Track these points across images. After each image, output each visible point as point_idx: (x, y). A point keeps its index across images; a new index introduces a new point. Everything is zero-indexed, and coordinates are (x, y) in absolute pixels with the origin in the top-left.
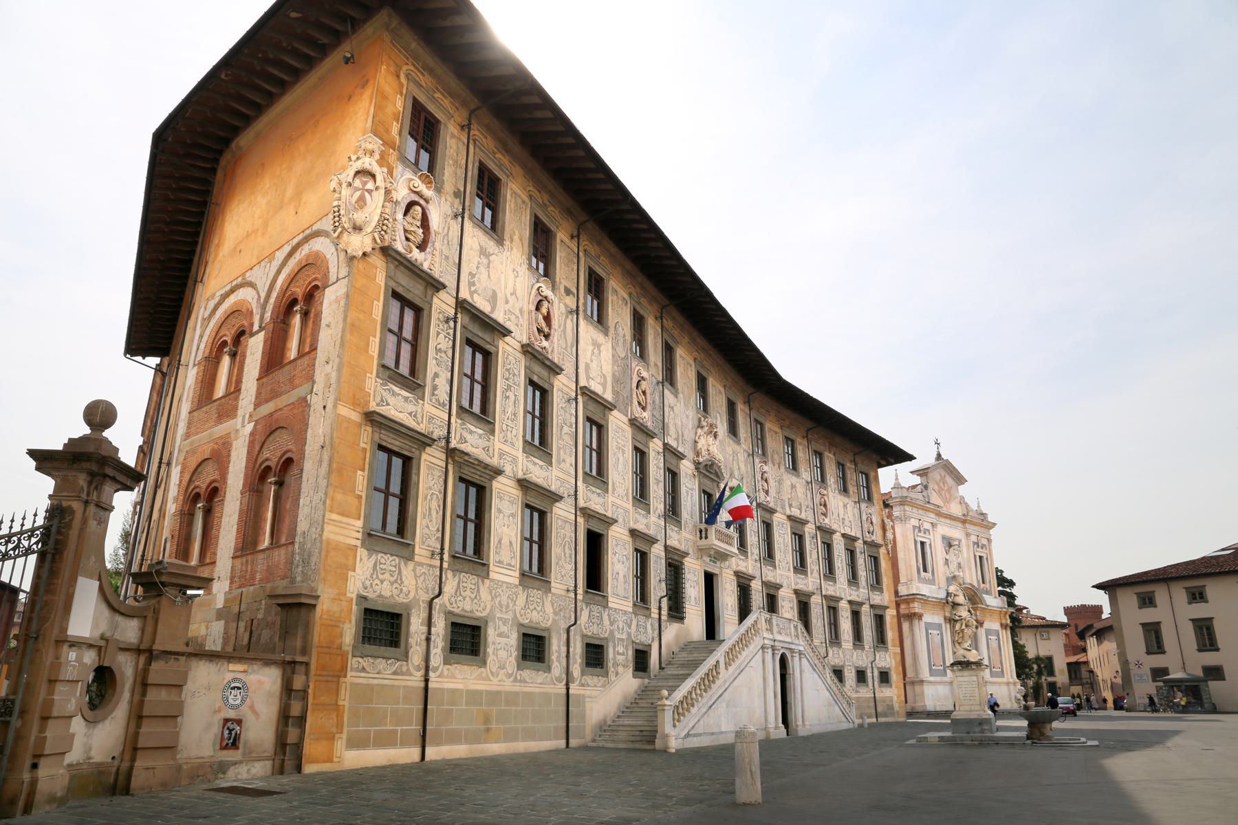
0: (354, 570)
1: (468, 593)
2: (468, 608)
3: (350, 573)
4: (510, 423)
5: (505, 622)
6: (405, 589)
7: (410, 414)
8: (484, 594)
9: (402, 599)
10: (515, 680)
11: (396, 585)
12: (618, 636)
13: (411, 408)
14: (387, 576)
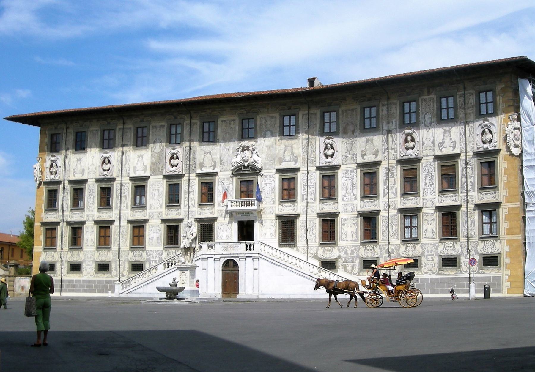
1: (75, 256)
5: (89, 261)
10: (95, 276)
12: (152, 259)
13: (55, 216)
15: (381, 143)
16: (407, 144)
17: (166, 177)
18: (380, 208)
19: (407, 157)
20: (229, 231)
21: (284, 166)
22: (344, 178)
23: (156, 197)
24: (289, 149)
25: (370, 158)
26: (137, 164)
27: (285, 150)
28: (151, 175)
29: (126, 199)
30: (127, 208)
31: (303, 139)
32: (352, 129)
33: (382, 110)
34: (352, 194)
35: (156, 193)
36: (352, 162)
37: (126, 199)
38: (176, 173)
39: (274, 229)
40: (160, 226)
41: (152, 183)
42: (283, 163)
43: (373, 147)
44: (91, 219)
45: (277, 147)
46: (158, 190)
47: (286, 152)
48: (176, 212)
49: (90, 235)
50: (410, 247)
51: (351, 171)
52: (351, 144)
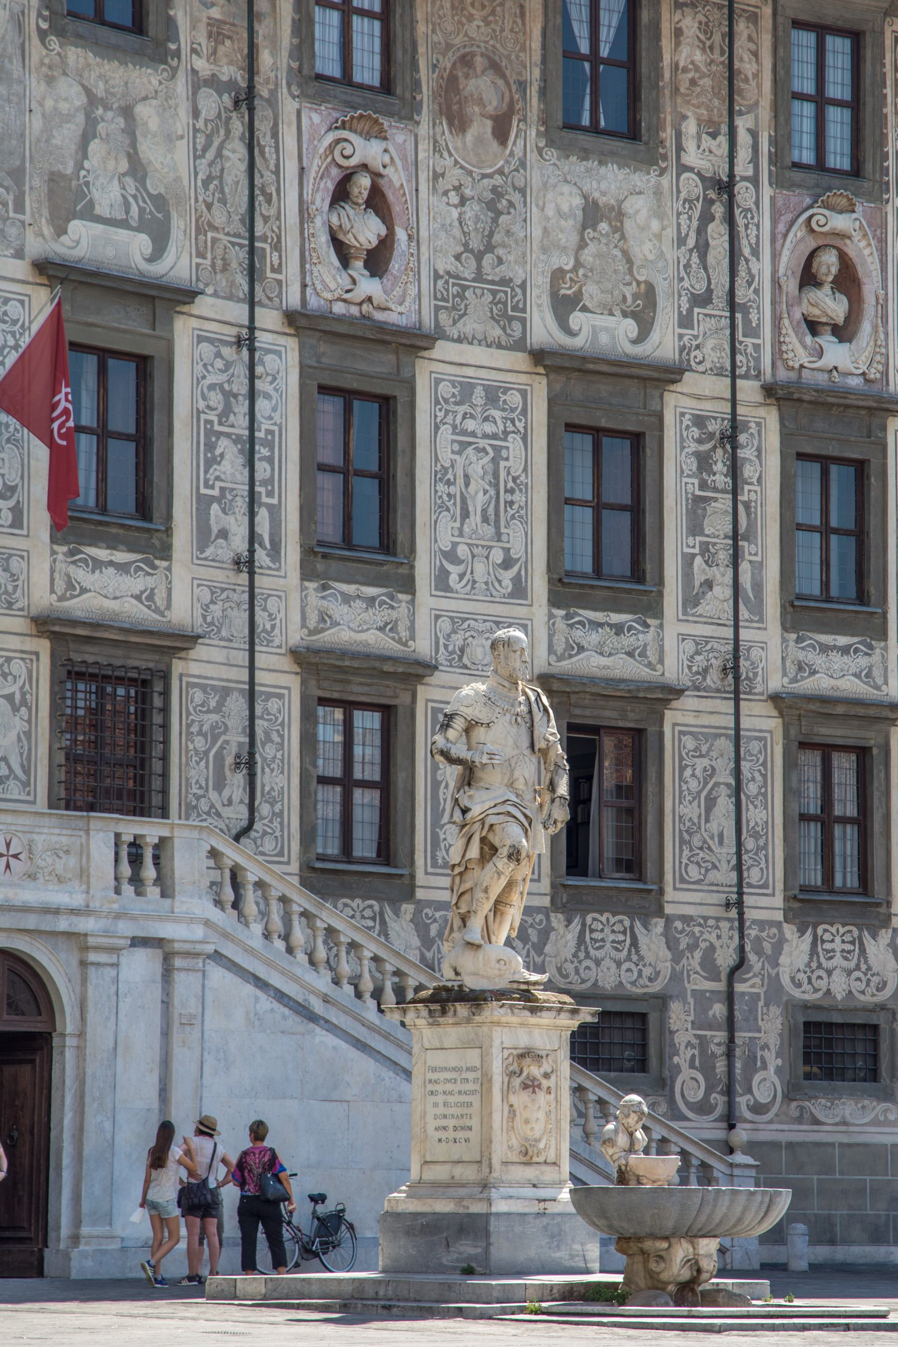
15: (671, 253)
16: (814, 294)
18: (672, 670)
19: (822, 379)
21: (83, 242)
22: (446, 432)
24: (111, 124)
25: (602, 331)
27: (91, 123)
31: (197, 83)
32: (493, 103)
33: (678, 33)
34: (497, 556)
36: (497, 332)
39: (18, 724)
42: (76, 227)
43: (622, 267)
45: (36, 86)
47: (94, 146)
50: (838, 945)
51: (493, 395)
52: (494, 205)
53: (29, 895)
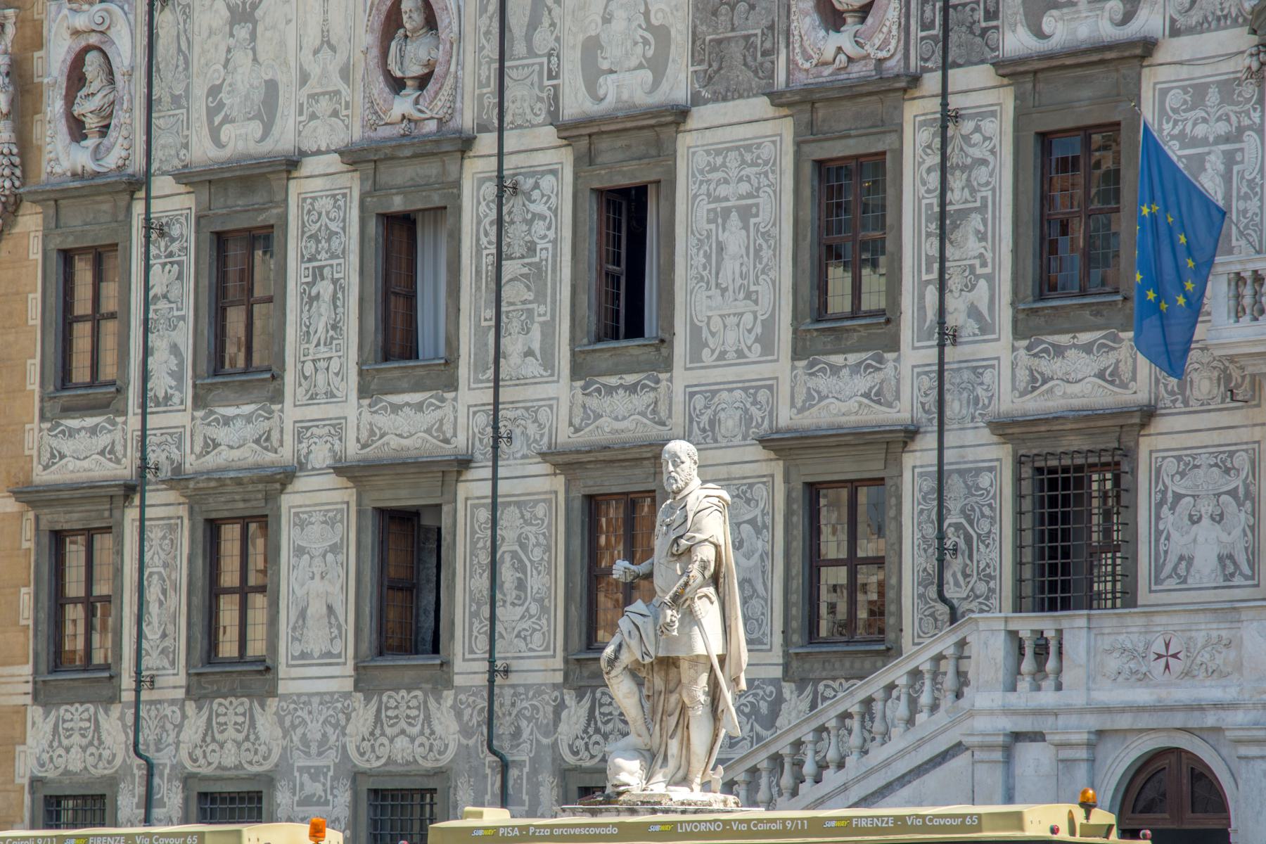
0: (24, 743)
1: (231, 732)
2: (229, 759)
3: (19, 748)
4: (323, 352)
5: (315, 774)
6: (106, 753)
7: (102, 453)
8: (266, 724)
9: (102, 770)
11: (92, 750)
13: (103, 440)
14: (76, 738)
17: (804, 103)
20: (1239, 518)
23: (730, 268)
26: (607, 20)
28: (697, 100)
29: (540, 297)
30: (548, 362)
35: (734, 238)
37: (540, 297)
38: (857, 71)
40: (760, 491)
41: (702, 160)
44: (321, 456)
46: (746, 214)
48: (863, 383)
49: (319, 576)
53: (1182, 694)
